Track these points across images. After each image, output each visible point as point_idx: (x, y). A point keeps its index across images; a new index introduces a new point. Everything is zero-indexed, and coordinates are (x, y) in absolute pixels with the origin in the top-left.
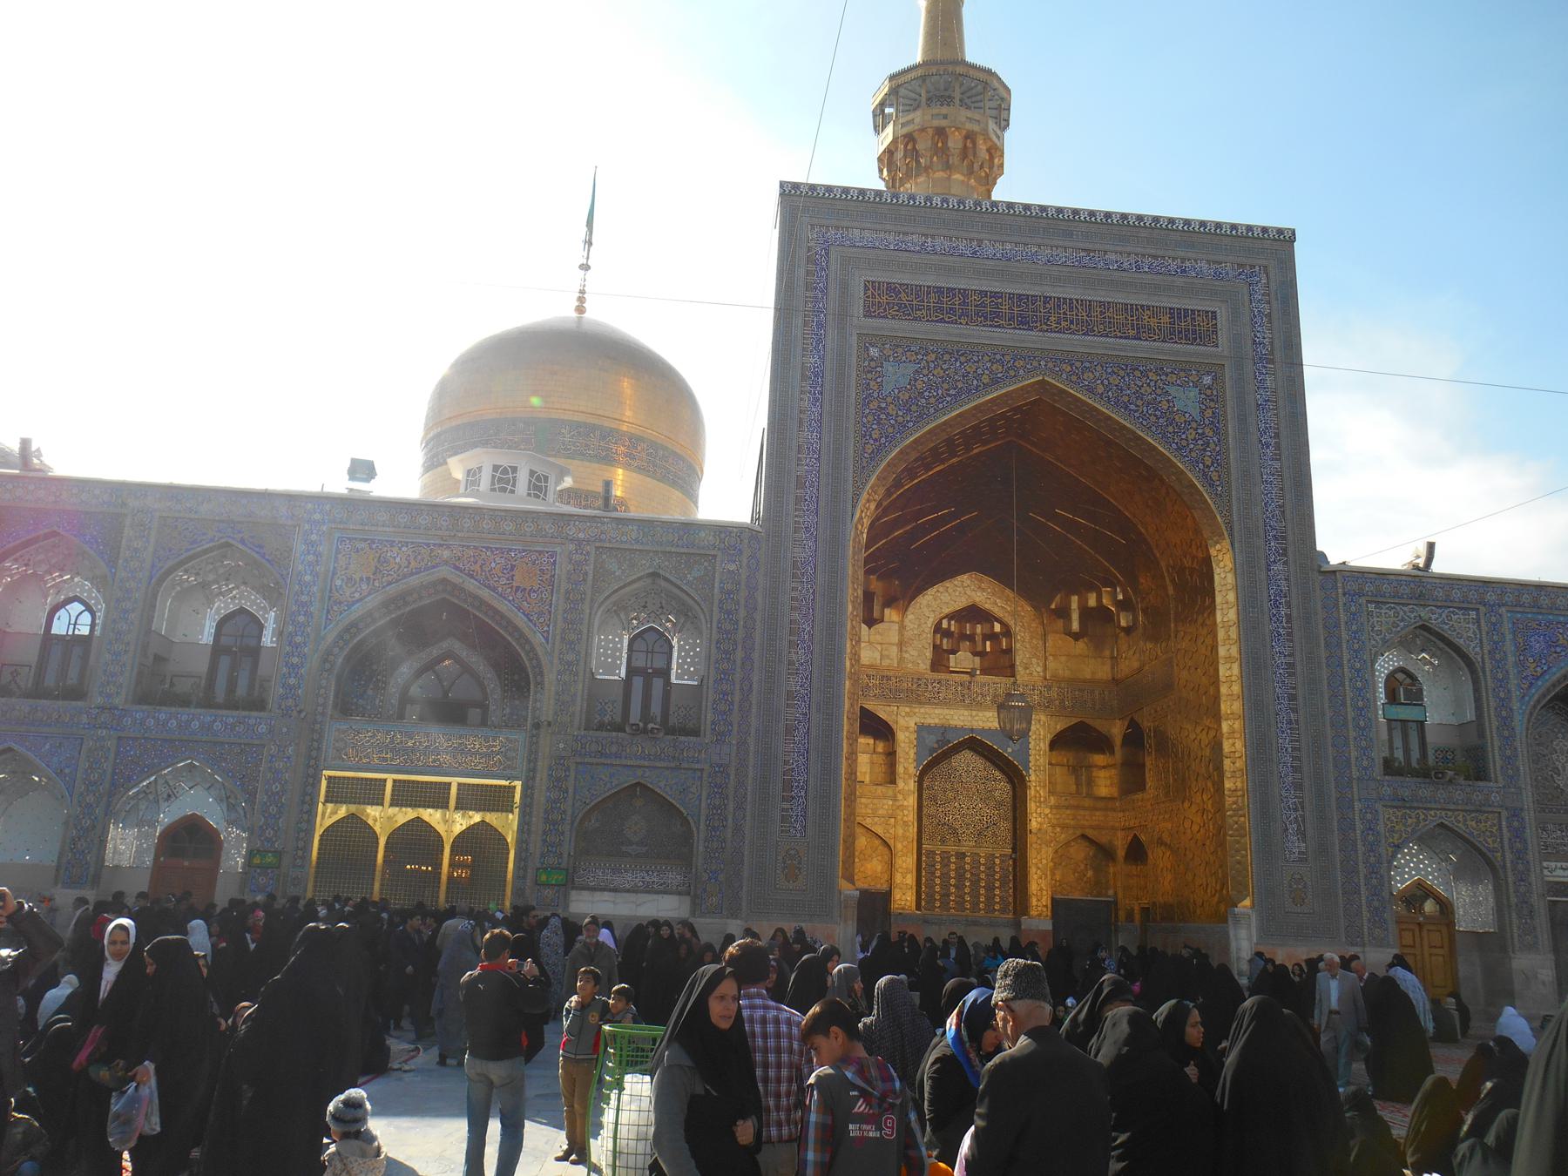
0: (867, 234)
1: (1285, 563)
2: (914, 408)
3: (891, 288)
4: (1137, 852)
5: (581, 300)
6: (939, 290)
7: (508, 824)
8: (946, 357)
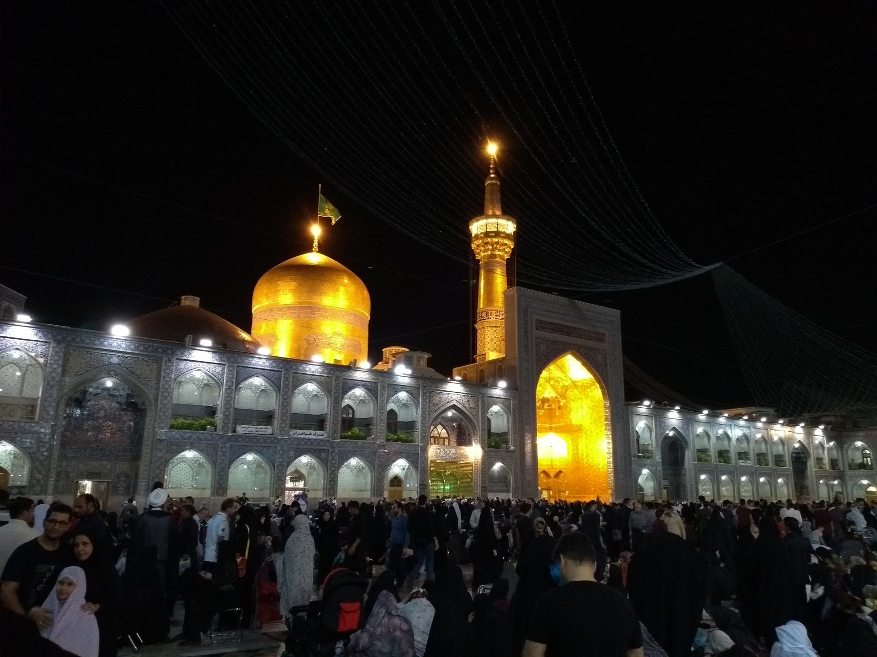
3: (541, 322)
6: (551, 323)
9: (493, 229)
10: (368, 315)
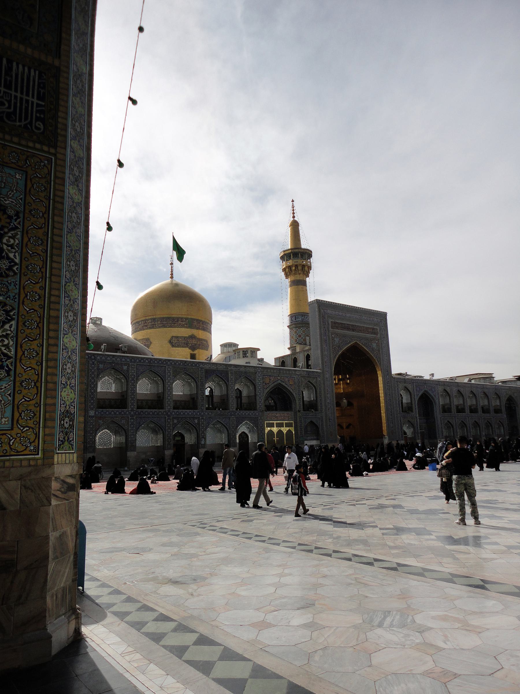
3: (335, 323)
4: (348, 427)
5: (172, 274)
7: (292, 429)
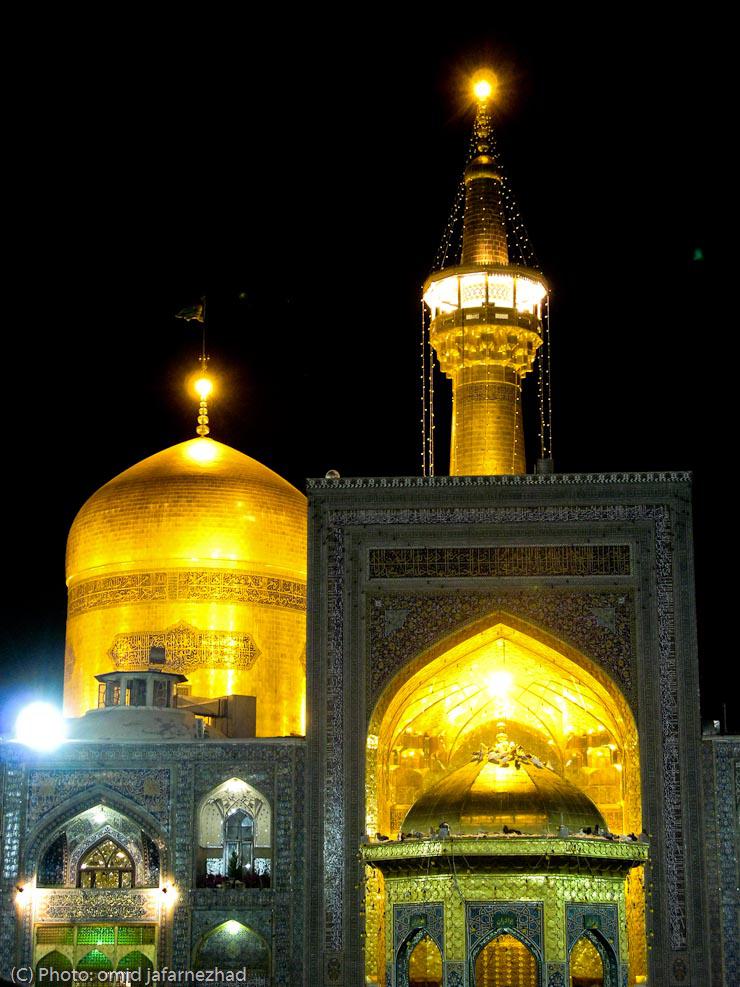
0: (370, 513)
1: (676, 736)
2: (407, 643)
3: (389, 554)
6: (423, 552)
8: (430, 602)
9: (484, 301)
10: (300, 571)
